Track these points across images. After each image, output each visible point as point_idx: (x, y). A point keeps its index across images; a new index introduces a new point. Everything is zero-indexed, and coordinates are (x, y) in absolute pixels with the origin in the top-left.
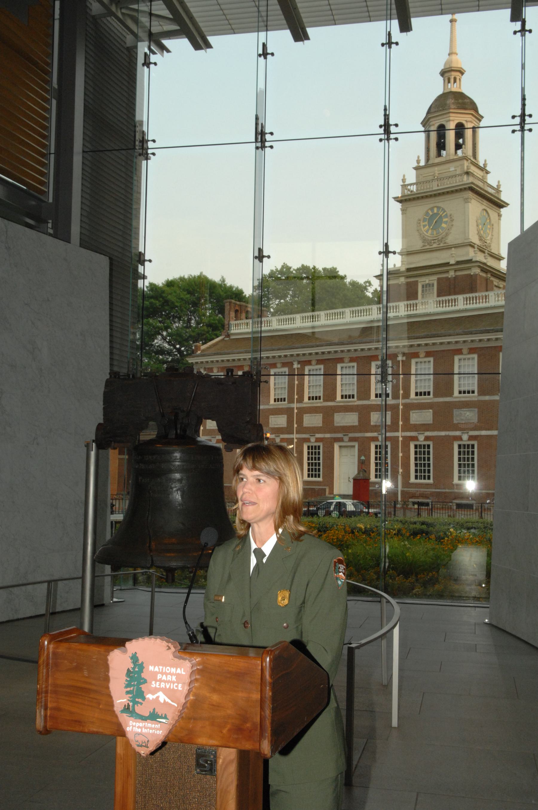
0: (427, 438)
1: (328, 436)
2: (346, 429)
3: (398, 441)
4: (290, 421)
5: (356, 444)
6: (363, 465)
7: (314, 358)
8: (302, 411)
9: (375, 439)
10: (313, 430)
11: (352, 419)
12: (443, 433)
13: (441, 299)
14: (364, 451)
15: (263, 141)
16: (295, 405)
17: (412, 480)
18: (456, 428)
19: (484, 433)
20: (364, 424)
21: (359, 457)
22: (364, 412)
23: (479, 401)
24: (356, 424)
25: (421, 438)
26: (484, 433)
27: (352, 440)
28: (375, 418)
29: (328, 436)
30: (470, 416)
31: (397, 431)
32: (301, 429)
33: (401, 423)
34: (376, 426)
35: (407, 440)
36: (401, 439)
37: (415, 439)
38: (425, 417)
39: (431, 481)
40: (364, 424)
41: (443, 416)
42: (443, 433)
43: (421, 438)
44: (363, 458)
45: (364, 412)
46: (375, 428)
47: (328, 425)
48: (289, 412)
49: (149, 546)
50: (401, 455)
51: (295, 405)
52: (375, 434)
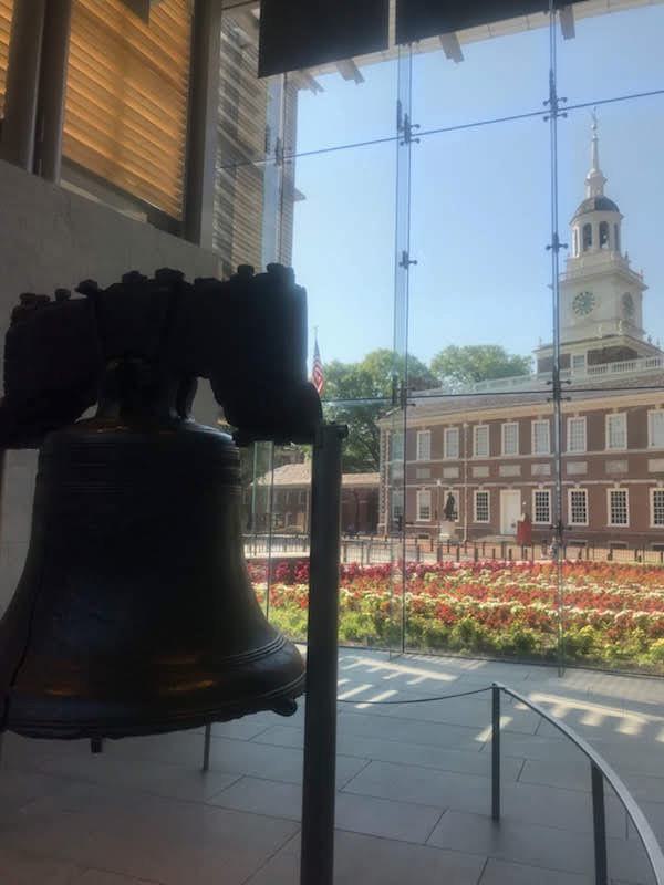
1: (494, 485)
2: (510, 480)
4: (461, 473)
6: (526, 510)
8: (472, 464)
9: (536, 487)
10: (481, 481)
11: (515, 471)
12: (596, 482)
13: (591, 367)
14: (525, 497)
15: (555, 109)
16: (464, 460)
18: (609, 478)
19: (634, 482)
20: (526, 474)
22: (526, 465)
23: (630, 454)
26: (634, 482)
27: (515, 488)
28: (535, 469)
29: (494, 485)
30: (622, 467)
32: (471, 479)
38: (581, 468)
40: (526, 474)
41: (597, 466)
42: (596, 482)
45: (526, 465)
46: (538, 478)
47: (494, 476)
48: (459, 465)
51: (464, 460)
52: (535, 484)
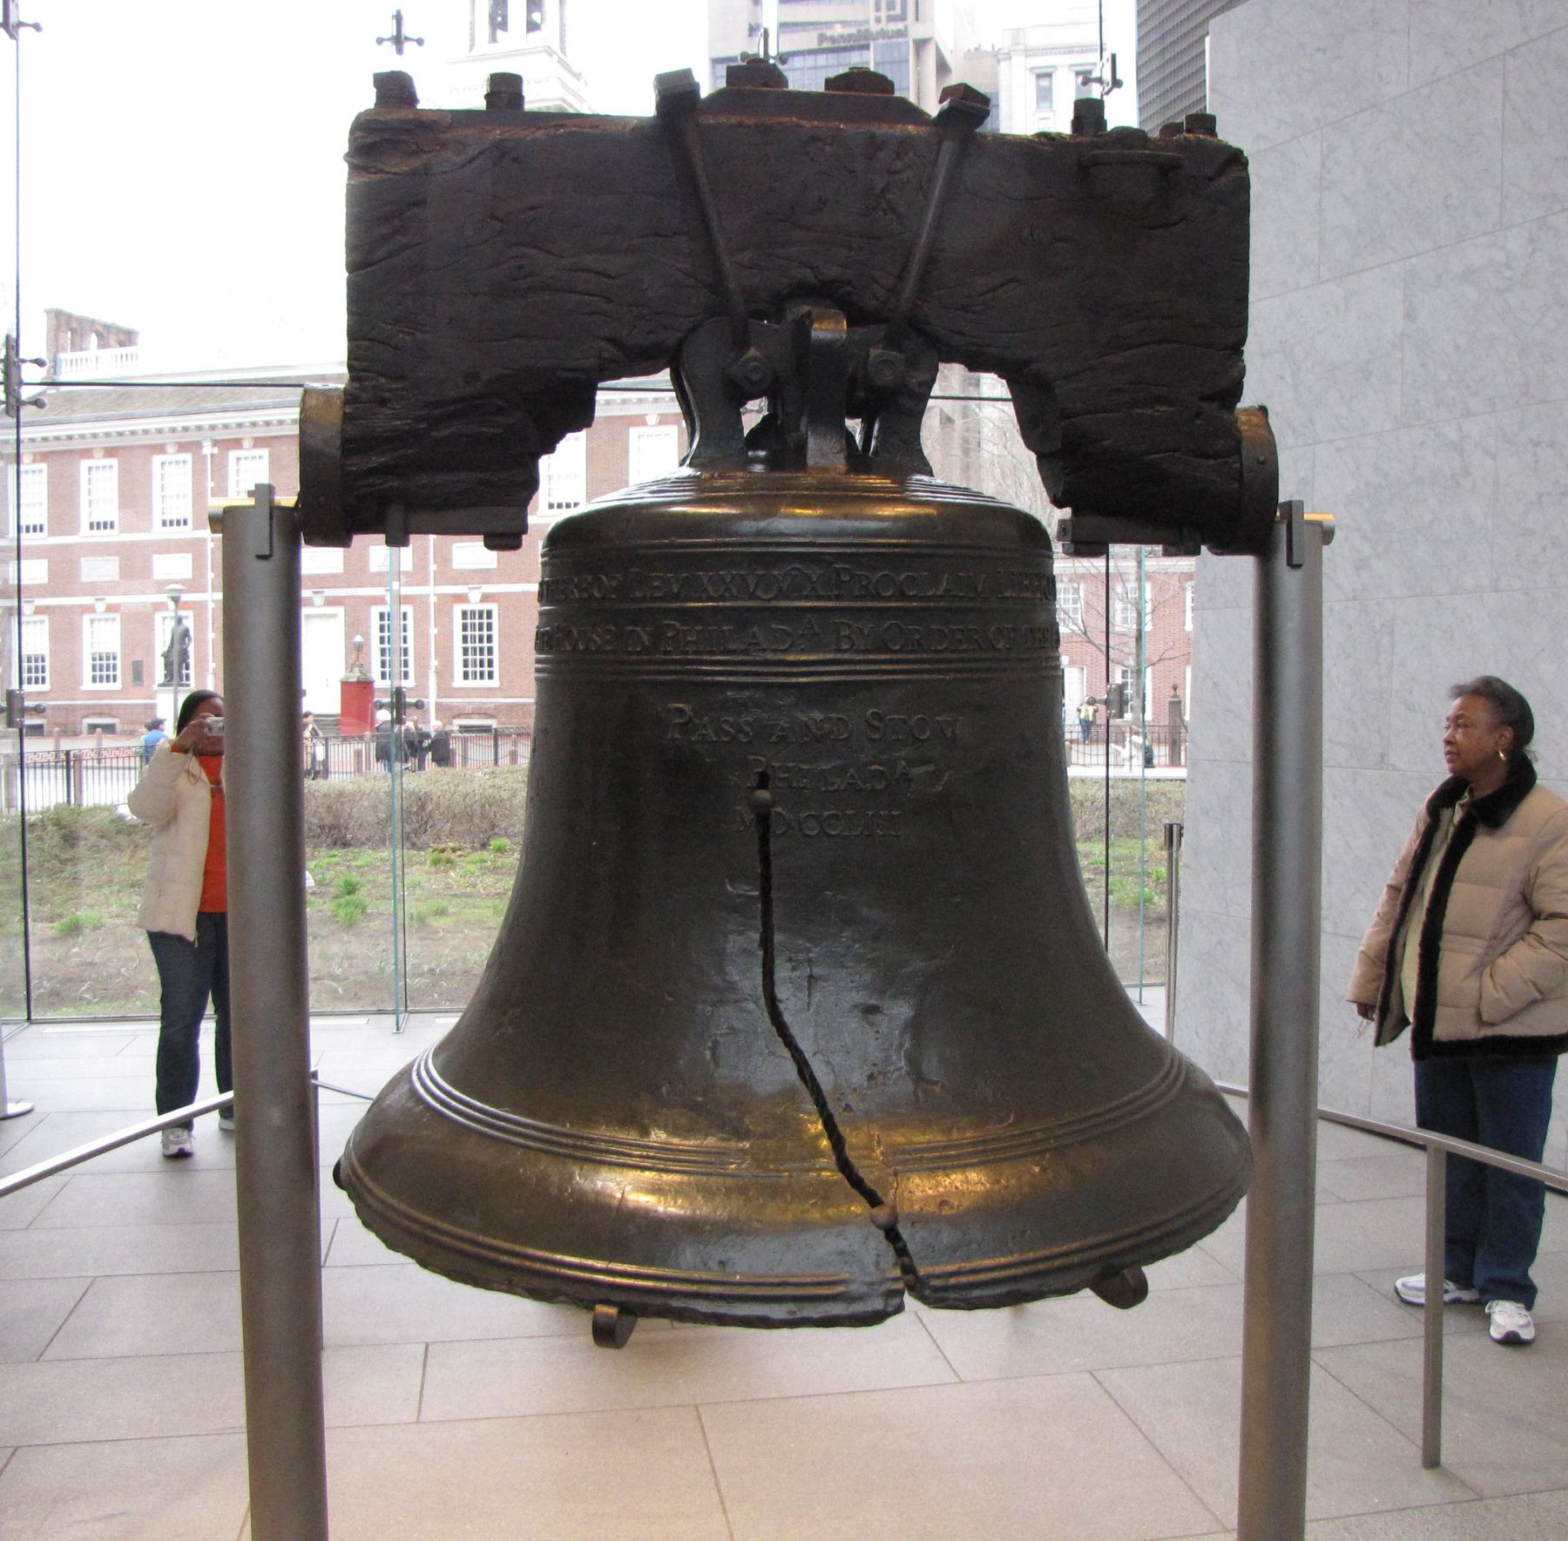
0: (486, 598)
3: (427, 605)
5: (340, 610)
6: (357, 652)
7: (247, 436)
9: (379, 600)
14: (355, 623)
17: (458, 681)
21: (349, 636)
24: (340, 569)
25: (475, 596)
27: (330, 602)
31: (425, 582)
33: (433, 567)
34: (380, 574)
35: (446, 602)
36: (433, 600)
37: (462, 598)
39: (495, 683)
43: (475, 596)
44: (359, 639)
46: (379, 579)
49: (845, 1166)
50: (433, 631)
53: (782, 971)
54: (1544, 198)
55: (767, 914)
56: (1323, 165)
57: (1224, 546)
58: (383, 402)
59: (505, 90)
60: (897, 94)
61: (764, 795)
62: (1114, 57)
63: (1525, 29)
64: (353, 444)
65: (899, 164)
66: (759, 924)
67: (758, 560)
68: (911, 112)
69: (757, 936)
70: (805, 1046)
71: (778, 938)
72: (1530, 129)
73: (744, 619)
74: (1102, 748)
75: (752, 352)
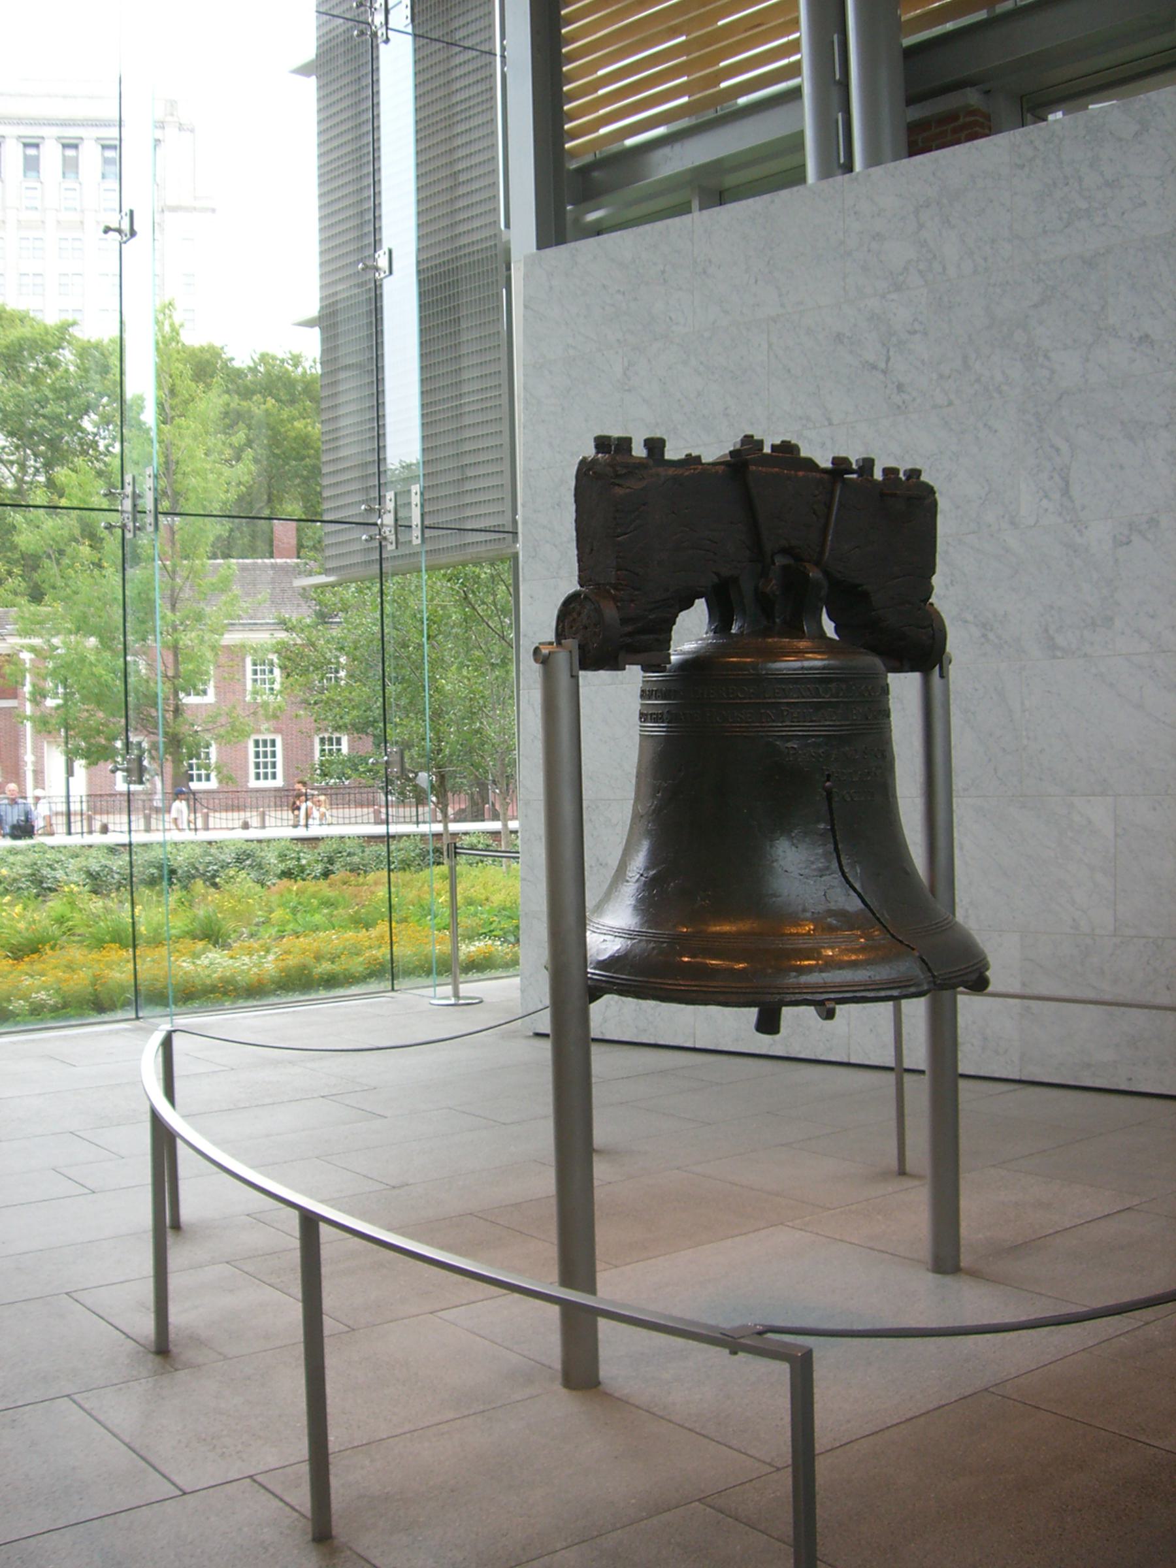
53: (844, 862)
54: (801, 418)
55: (834, 837)
56: (625, 374)
57: (912, 669)
58: (632, 601)
59: (655, 446)
60: (803, 454)
61: (828, 784)
62: (390, 252)
63: (783, 306)
64: (624, 621)
65: (817, 492)
66: (831, 840)
67: (822, 681)
68: (810, 464)
69: (832, 846)
70: (860, 890)
71: (840, 847)
72: (789, 371)
73: (818, 706)
74: (125, 818)
75: (774, 582)
